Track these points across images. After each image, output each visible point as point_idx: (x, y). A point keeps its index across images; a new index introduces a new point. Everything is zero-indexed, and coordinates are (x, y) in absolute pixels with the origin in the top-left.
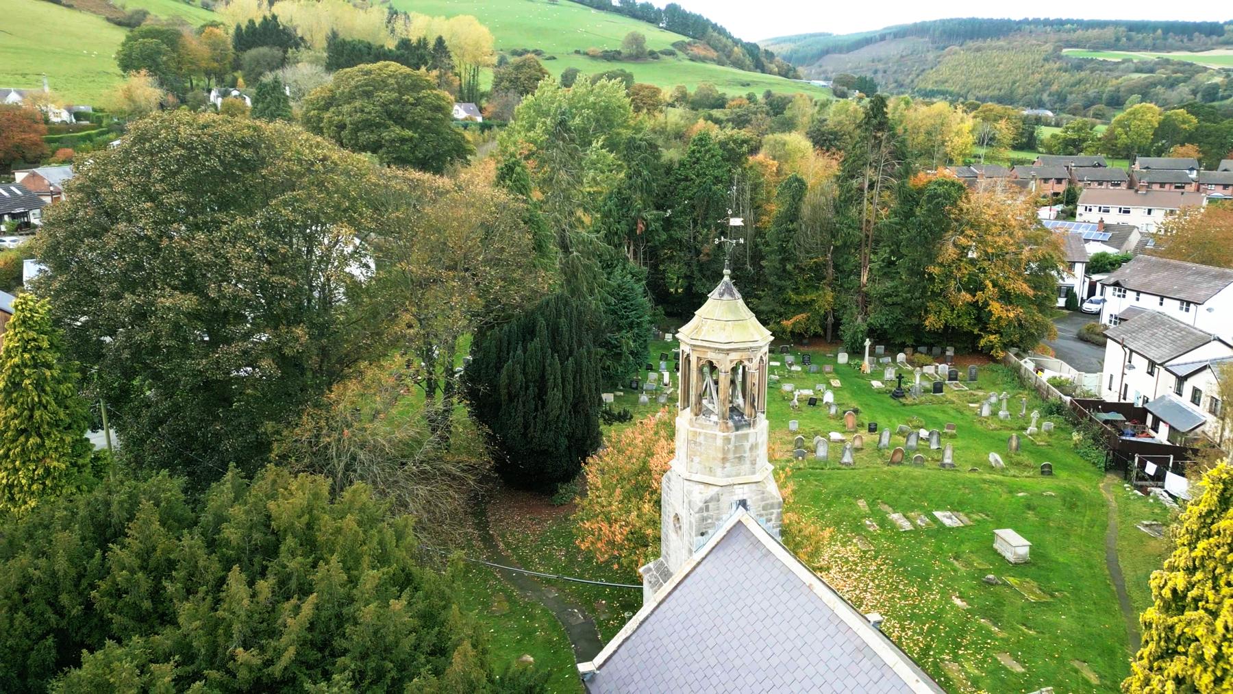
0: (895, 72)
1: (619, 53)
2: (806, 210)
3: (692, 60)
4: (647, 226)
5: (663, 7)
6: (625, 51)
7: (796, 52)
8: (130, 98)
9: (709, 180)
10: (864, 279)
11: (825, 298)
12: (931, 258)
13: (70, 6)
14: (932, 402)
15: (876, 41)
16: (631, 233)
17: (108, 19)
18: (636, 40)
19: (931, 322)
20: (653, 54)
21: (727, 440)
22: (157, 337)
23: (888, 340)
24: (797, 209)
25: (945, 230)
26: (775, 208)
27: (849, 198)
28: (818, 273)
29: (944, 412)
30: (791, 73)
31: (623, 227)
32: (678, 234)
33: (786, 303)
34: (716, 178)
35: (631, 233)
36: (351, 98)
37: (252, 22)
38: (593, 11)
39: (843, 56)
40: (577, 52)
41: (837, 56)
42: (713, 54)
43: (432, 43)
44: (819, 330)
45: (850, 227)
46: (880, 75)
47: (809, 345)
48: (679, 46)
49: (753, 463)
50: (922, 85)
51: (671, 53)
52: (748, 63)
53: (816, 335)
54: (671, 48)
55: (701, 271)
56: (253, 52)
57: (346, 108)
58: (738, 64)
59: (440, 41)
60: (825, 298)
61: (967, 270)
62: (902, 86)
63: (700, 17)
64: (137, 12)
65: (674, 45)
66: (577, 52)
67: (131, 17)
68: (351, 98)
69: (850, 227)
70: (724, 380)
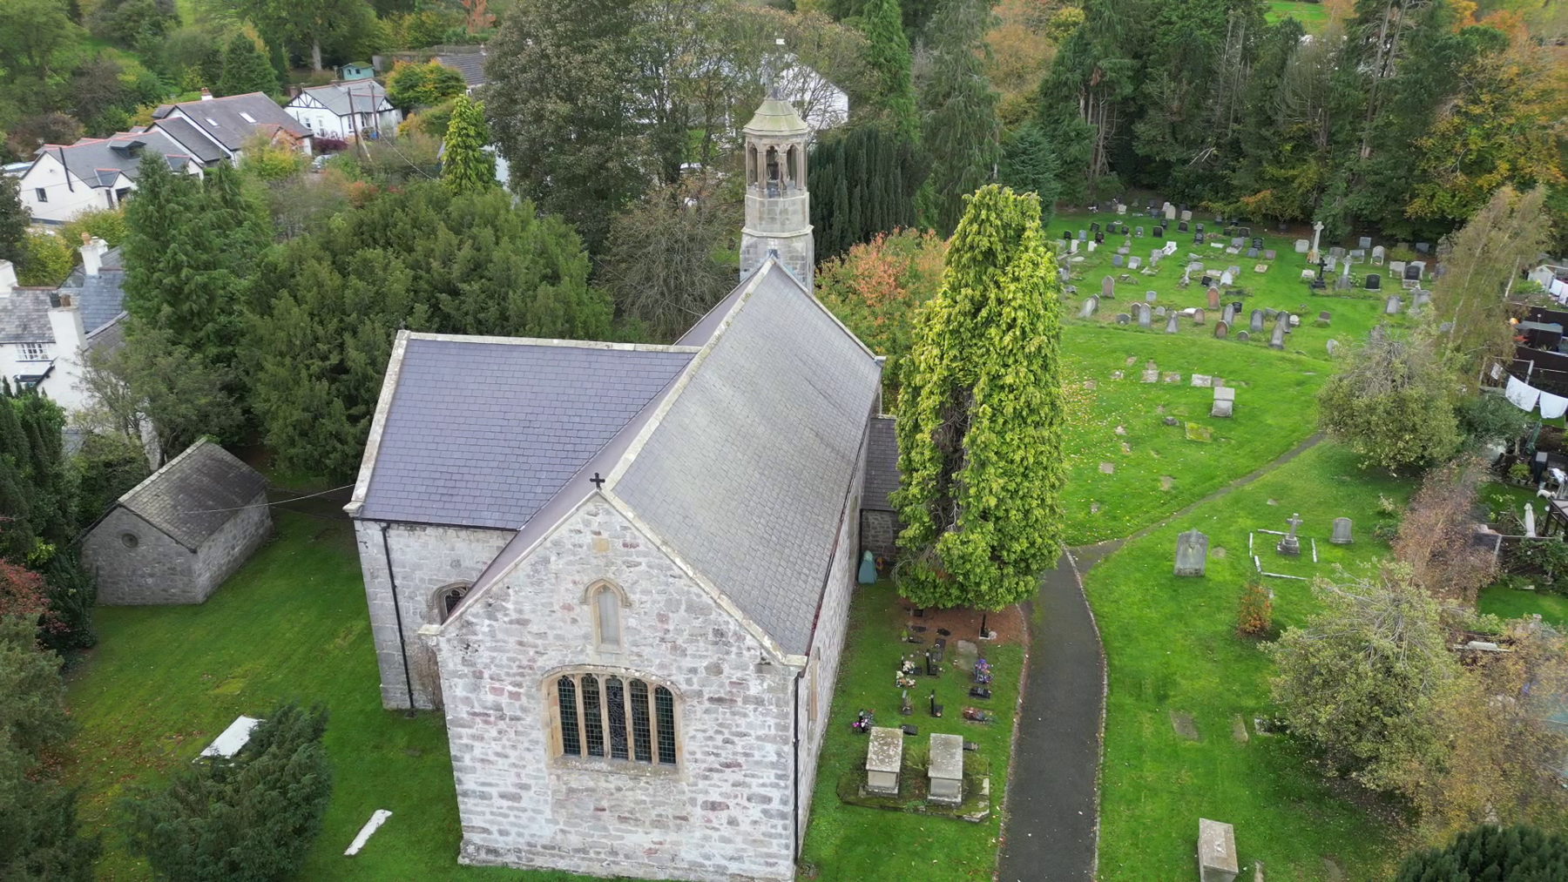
2: (1293, 62)
4: (1103, 76)
9: (1193, 23)
10: (1366, 152)
14: (1353, 297)
16: (1086, 82)
19: (1415, 208)
21: (762, 204)
22: (544, 135)
24: (1284, 62)
25: (1455, 91)
27: (1356, 52)
28: (1304, 143)
29: (1354, 307)
31: (1077, 76)
32: (1150, 88)
33: (1260, 177)
34: (1205, 21)
35: (1086, 82)
44: (1297, 213)
45: (1349, 85)
47: (1288, 231)
49: (783, 224)
53: (1293, 220)
55: (1174, 133)
60: (1309, 171)
61: (1476, 143)
69: (1349, 85)
70: (762, 161)
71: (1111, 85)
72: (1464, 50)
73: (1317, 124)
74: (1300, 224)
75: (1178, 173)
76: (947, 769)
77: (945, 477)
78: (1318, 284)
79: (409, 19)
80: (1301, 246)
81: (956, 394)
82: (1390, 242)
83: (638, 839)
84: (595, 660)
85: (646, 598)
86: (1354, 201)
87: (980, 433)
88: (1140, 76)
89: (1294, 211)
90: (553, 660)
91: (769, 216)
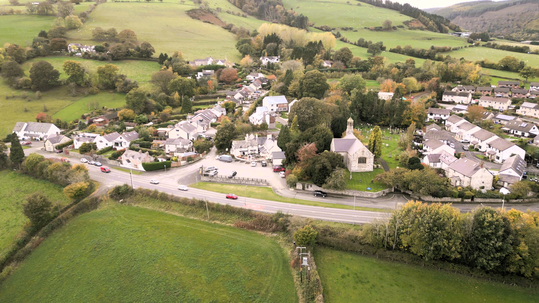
0: (518, 21)
1: (381, 28)
3: (410, 29)
5: (403, 5)
6: (384, 27)
7: (471, 10)
8: (247, 63)
11: (388, 119)
12: (402, 114)
13: (212, 24)
15: (511, 6)
17: (223, 27)
18: (388, 23)
19: (402, 124)
20: (394, 28)
23: (396, 126)
26: (381, 104)
30: (457, 29)
32: (364, 107)
36: (309, 78)
37: (268, 35)
38: (374, 7)
39: (493, 12)
40: (365, 28)
41: (491, 12)
42: (421, 25)
43: (318, 42)
46: (510, 22)
48: (407, 23)
50: (529, 28)
51: (401, 27)
52: (435, 27)
54: (402, 24)
56: (269, 45)
57: (308, 80)
58: (430, 29)
59: (320, 42)
60: (388, 119)
61: (408, 116)
62: (520, 27)
63: (417, 9)
64: (230, 25)
65: (404, 23)
66: (365, 28)
67: (228, 26)
68: (309, 78)
71: (359, 107)
72: (406, 105)
73: (388, 112)
74: (388, 126)
75: (369, 119)
76: (379, 165)
77: (374, 148)
78: (392, 133)
79: (199, 88)
80: (388, 129)
81: (375, 141)
82: (399, 128)
83: (363, 169)
84: (362, 156)
85: (366, 152)
86: (395, 123)
87: (377, 144)
88: (363, 106)
89: (386, 124)
90: (359, 156)
91: (350, 128)
